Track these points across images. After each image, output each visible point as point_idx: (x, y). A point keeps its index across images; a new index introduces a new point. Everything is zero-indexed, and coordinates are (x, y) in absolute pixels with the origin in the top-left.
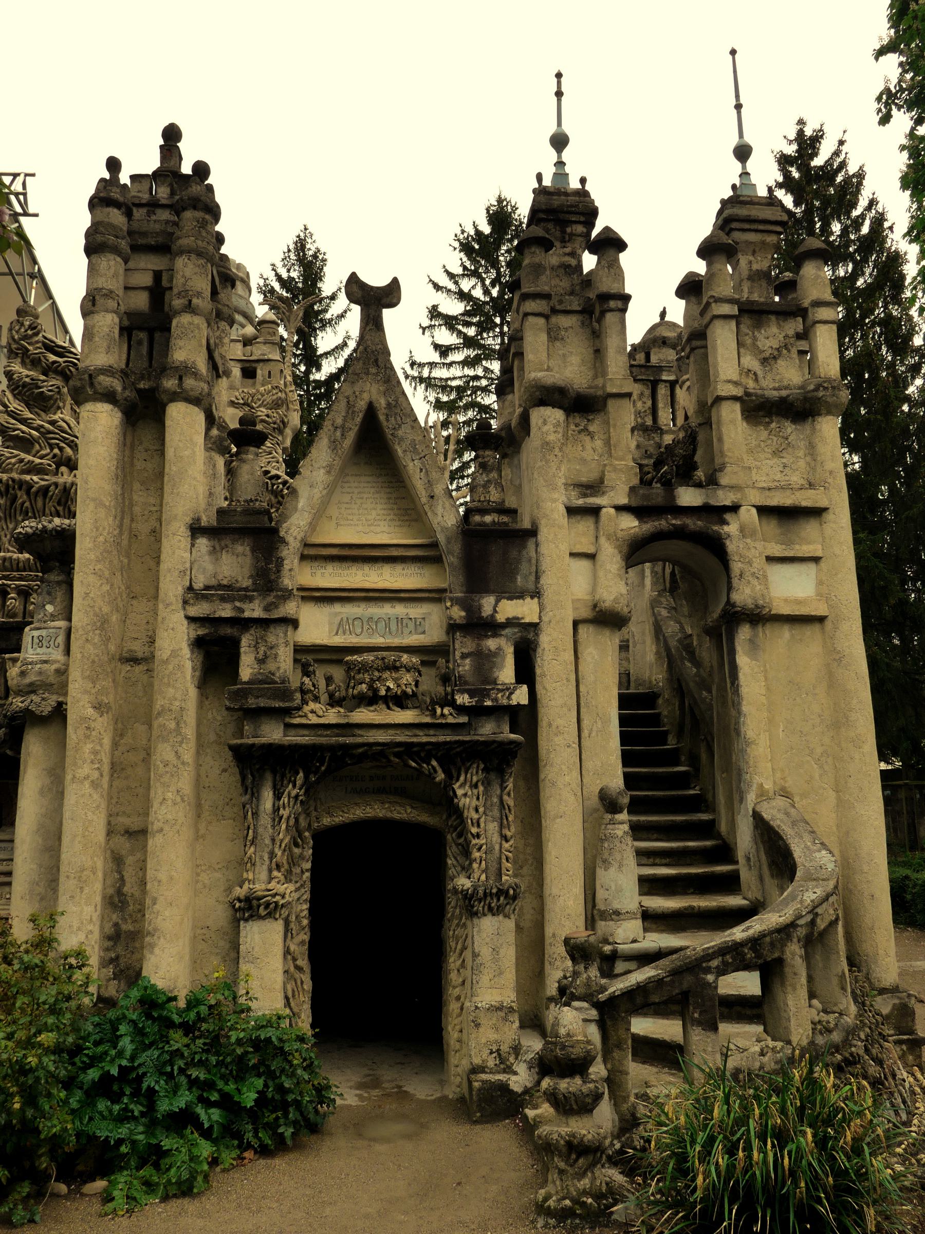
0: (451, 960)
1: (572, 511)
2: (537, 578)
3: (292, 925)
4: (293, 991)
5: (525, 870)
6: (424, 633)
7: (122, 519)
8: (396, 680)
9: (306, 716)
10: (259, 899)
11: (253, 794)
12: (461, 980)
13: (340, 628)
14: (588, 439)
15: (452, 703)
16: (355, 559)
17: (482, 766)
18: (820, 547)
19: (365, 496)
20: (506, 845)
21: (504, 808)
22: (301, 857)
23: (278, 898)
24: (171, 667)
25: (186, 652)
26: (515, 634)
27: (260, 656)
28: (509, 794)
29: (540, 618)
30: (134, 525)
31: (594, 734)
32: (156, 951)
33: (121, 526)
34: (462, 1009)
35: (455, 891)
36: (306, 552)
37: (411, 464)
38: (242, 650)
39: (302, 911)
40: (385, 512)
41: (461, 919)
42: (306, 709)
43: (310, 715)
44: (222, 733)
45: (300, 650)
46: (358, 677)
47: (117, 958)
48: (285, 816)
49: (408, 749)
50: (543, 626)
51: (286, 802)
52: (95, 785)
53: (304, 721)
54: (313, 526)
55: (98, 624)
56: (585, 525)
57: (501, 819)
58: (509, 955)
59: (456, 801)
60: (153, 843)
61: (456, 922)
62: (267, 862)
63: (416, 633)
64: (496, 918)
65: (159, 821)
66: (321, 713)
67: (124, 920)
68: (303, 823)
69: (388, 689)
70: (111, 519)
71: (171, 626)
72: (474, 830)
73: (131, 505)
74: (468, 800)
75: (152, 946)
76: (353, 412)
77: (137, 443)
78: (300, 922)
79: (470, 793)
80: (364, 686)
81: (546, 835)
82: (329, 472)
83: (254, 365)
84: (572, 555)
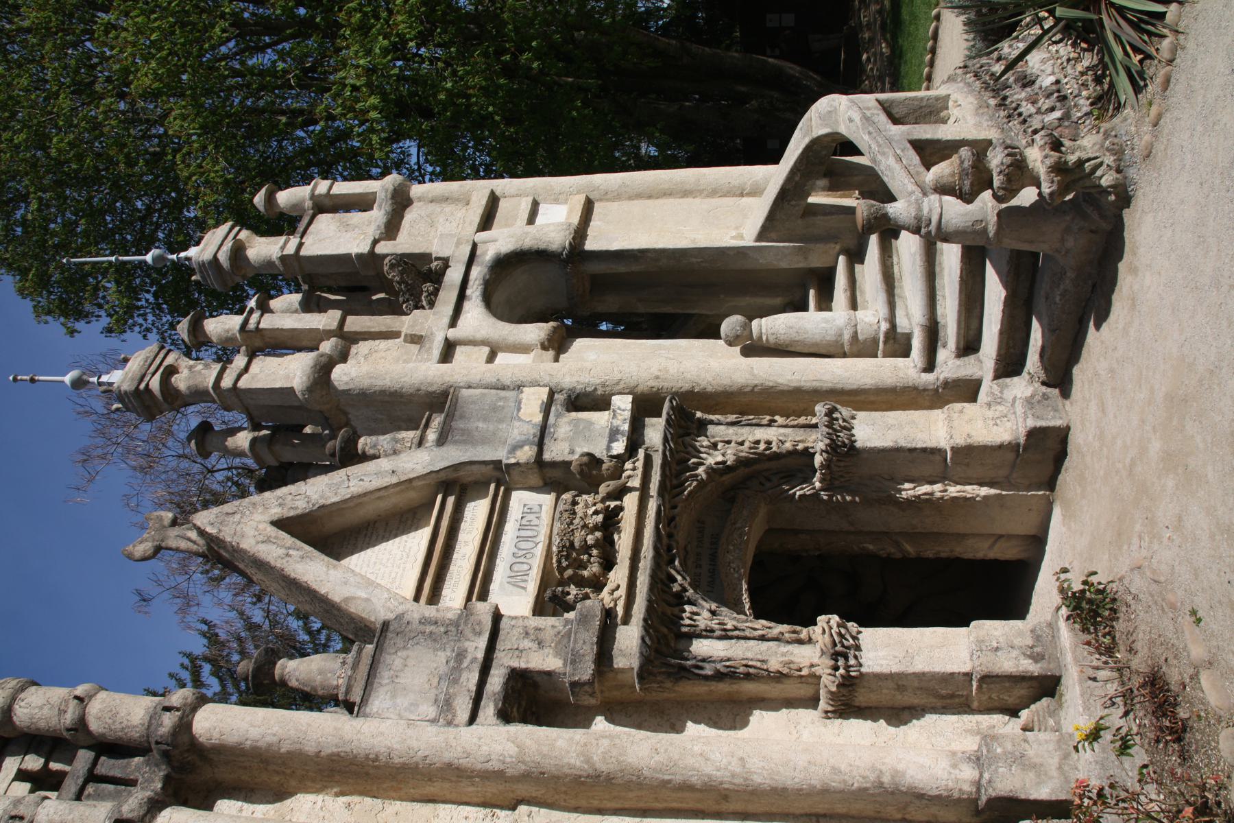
6: (541, 506)
10: (835, 644)
18: (524, 199)
21: (741, 421)
27: (535, 646)
29: (545, 386)
32: (901, 767)
37: (352, 489)
38: (523, 666)
65: (730, 763)
69: (596, 513)
71: (475, 740)
72: (762, 446)
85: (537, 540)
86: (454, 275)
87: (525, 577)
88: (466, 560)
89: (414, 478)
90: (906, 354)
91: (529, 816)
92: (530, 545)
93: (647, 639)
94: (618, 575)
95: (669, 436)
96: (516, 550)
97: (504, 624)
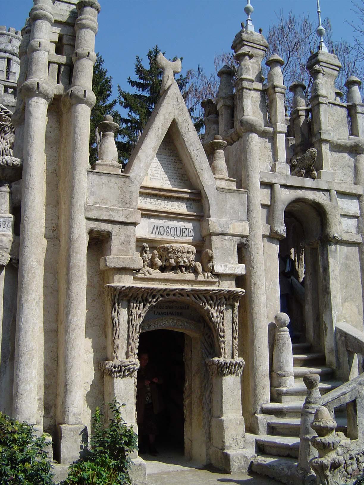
8: (187, 258)
17: (225, 302)
21: (234, 324)
26: (238, 240)
29: (250, 233)
37: (193, 152)
38: (113, 237)
40: (173, 175)
42: (145, 270)
44: (92, 281)
48: (135, 325)
49: (188, 293)
51: (135, 317)
53: (143, 276)
57: (233, 328)
62: (125, 348)
63: (189, 236)
65: (73, 324)
69: (184, 262)
72: (222, 334)
74: (219, 319)
85: (176, 236)
86: (309, 182)
87: (157, 233)
88: (164, 206)
89: (200, 179)
90: (272, 400)
91: (53, 245)
92: (173, 234)
93: (124, 288)
94: (157, 274)
95: (222, 292)
96: (170, 228)
97: (130, 227)
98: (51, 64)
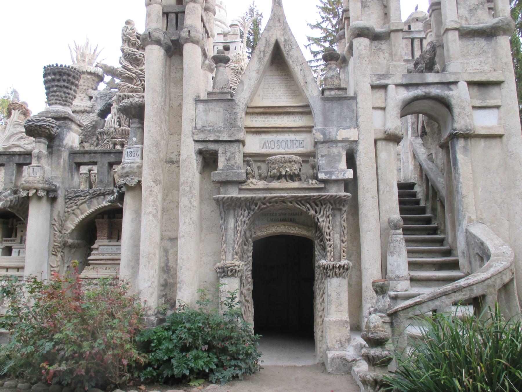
0: (318, 299)
1: (374, 87)
2: (357, 119)
3: (244, 281)
4: (244, 311)
5: (352, 258)
6: (303, 147)
7: (165, 98)
8: (290, 167)
9: (248, 185)
10: (228, 268)
11: (225, 220)
12: (322, 308)
13: (264, 145)
14: (381, 53)
15: (316, 178)
16: (270, 114)
17: (331, 207)
18: (500, 101)
19: (275, 85)
20: (344, 245)
22: (247, 250)
23: (236, 267)
24: (187, 163)
25: (194, 156)
26: (347, 145)
27: (227, 158)
28: (344, 221)
29: (358, 138)
30: (171, 102)
31: (385, 193)
32: (182, 290)
33: (165, 101)
34: (323, 321)
35: (319, 267)
36: (248, 111)
39: (248, 275)
41: (322, 280)
42: (249, 181)
43: (250, 184)
45: (245, 155)
46: (272, 166)
47: (166, 294)
49: (297, 199)
50: (360, 141)
52: (154, 216)
53: (248, 187)
54: (251, 99)
55: (155, 144)
56: (380, 93)
58: (345, 296)
59: (319, 224)
60: (180, 242)
61: (319, 281)
62: (232, 251)
63: (300, 147)
64: (338, 279)
66: (255, 183)
67: (169, 277)
68: (248, 234)
69: (287, 172)
70: (160, 98)
73: (170, 93)
74: (324, 223)
75: (180, 288)
76: (269, 44)
77: (172, 65)
78: (247, 280)
79: (325, 220)
80: (275, 170)
81: (362, 240)
82: (258, 73)
83: (228, 44)
84: (374, 108)
94: (262, 184)
95: (324, 197)
98: (169, 15)
